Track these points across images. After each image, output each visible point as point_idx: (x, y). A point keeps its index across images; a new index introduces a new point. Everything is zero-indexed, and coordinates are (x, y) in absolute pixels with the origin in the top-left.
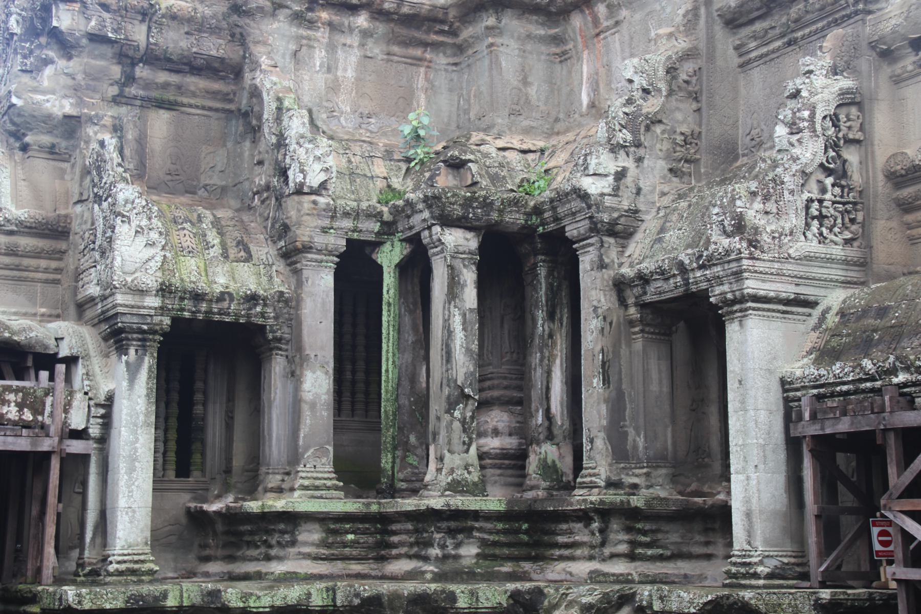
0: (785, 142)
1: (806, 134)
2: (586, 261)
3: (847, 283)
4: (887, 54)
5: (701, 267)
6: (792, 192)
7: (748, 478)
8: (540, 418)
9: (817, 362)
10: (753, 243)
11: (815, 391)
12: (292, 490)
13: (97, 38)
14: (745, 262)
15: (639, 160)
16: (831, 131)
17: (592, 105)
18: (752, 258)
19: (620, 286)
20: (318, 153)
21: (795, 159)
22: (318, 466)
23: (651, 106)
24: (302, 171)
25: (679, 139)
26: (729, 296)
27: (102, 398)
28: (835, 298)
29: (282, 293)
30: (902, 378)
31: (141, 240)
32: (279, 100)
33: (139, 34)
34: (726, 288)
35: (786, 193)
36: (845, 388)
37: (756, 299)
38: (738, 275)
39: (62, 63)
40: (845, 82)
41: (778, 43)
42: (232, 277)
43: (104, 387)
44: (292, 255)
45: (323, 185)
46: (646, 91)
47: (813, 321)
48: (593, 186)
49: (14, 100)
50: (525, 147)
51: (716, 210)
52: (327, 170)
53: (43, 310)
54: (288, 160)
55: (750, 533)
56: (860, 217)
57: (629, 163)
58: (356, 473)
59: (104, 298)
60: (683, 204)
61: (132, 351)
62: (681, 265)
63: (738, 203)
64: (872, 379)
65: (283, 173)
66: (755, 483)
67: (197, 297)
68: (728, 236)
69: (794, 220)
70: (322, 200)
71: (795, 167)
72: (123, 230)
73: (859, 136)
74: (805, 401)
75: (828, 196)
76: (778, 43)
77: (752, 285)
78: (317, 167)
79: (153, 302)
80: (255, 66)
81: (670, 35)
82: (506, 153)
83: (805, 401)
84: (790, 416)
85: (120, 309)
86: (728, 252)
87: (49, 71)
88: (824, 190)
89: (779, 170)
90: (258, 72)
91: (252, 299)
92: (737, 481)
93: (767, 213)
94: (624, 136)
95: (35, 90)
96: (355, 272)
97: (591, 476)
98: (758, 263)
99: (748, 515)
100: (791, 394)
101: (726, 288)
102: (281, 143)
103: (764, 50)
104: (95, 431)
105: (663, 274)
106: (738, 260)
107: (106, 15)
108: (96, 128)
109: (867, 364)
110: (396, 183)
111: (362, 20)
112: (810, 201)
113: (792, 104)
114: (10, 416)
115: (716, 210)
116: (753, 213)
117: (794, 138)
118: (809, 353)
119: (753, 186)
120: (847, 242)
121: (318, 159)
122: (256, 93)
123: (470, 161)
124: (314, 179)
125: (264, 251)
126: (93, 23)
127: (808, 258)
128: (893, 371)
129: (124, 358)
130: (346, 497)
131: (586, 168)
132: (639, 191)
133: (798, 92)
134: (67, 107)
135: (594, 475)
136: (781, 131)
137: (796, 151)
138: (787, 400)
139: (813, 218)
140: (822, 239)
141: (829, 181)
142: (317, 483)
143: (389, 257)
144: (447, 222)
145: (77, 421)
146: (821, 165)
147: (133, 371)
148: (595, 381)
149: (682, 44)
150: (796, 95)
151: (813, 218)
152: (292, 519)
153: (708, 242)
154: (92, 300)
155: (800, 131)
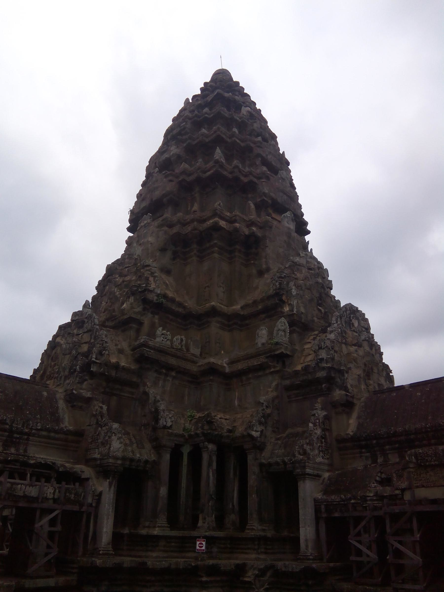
0: (312, 428)
1: (318, 427)
2: (250, 458)
3: (328, 471)
4: (334, 405)
5: (291, 463)
6: (317, 444)
7: (306, 529)
8: (231, 507)
9: (324, 494)
10: (309, 458)
11: (325, 503)
12: (155, 527)
13: (102, 374)
14: (307, 464)
15: (266, 427)
16: (323, 427)
17: (239, 405)
18: (308, 462)
19: (261, 465)
20: (170, 416)
21: (316, 433)
22: (162, 520)
23: (268, 411)
24: (166, 421)
25: (275, 422)
26: (300, 473)
27: (98, 492)
28: (326, 475)
29: (154, 460)
30: (353, 501)
31: (118, 441)
32: (155, 397)
33: (113, 373)
34: (298, 470)
35: (315, 444)
36: (335, 503)
37: (308, 474)
38: (304, 467)
39: (90, 381)
40: (325, 413)
41: (301, 398)
42: (146, 454)
43: (100, 489)
44: (158, 448)
45: (171, 426)
46: (267, 407)
47: (321, 481)
48: (254, 434)
49: (74, 391)
50: (225, 418)
51: (297, 447)
52: (172, 422)
53: (72, 460)
54: (159, 417)
55: (307, 546)
56: (330, 451)
57: (263, 428)
58: (173, 522)
59: (101, 459)
60: (279, 442)
61: (111, 478)
62: (284, 462)
63: (305, 446)
64: (344, 501)
65: (157, 420)
66: (307, 532)
67: (132, 460)
68: (301, 455)
69: (317, 452)
70: (170, 431)
71: (316, 436)
72: (113, 437)
73: (328, 428)
74: (323, 507)
75: (323, 445)
76: (301, 398)
77: (308, 471)
78: (169, 420)
79: (119, 462)
80: (145, 385)
81: (272, 391)
82: (221, 420)
83: (323, 507)
84: (317, 510)
85: (111, 464)
86: (301, 460)
87: (85, 383)
88: (322, 443)
89: (312, 437)
90: (146, 387)
91: (146, 462)
92: (302, 531)
93: (310, 449)
94: (263, 420)
95: (81, 389)
96: (176, 454)
97: (252, 526)
98: (309, 464)
99: (306, 540)
100: (317, 504)
101: (298, 470)
102: (157, 411)
103: (297, 398)
104: (94, 505)
105: (277, 463)
106: (305, 463)
107: (106, 367)
108: (98, 402)
109: (343, 496)
110: (187, 425)
111: (173, 374)
112: (320, 446)
113: (312, 418)
114: (72, 498)
115: (297, 447)
116: (307, 448)
117: (315, 428)
118: (321, 491)
119: (308, 441)
120: (328, 459)
121: (170, 418)
122: (146, 394)
123: (214, 422)
124: (169, 424)
125: (148, 446)
126: (102, 370)
127: (320, 463)
128: (350, 499)
129: (108, 480)
130: (171, 530)
131: (253, 429)
132: (266, 437)
133: (315, 414)
134: (89, 395)
135: (253, 526)
136: (311, 425)
137: (316, 431)
138: (315, 505)
139: (320, 451)
140: (323, 458)
141: (323, 440)
142: (163, 525)
143: (186, 450)
144: (210, 441)
145: (90, 500)
146: (321, 436)
147: (110, 484)
148: (254, 496)
149: (275, 394)
150: (314, 415)
151: (320, 451)
152: (157, 538)
153: (294, 456)
154: (95, 459)
155: (316, 426)
